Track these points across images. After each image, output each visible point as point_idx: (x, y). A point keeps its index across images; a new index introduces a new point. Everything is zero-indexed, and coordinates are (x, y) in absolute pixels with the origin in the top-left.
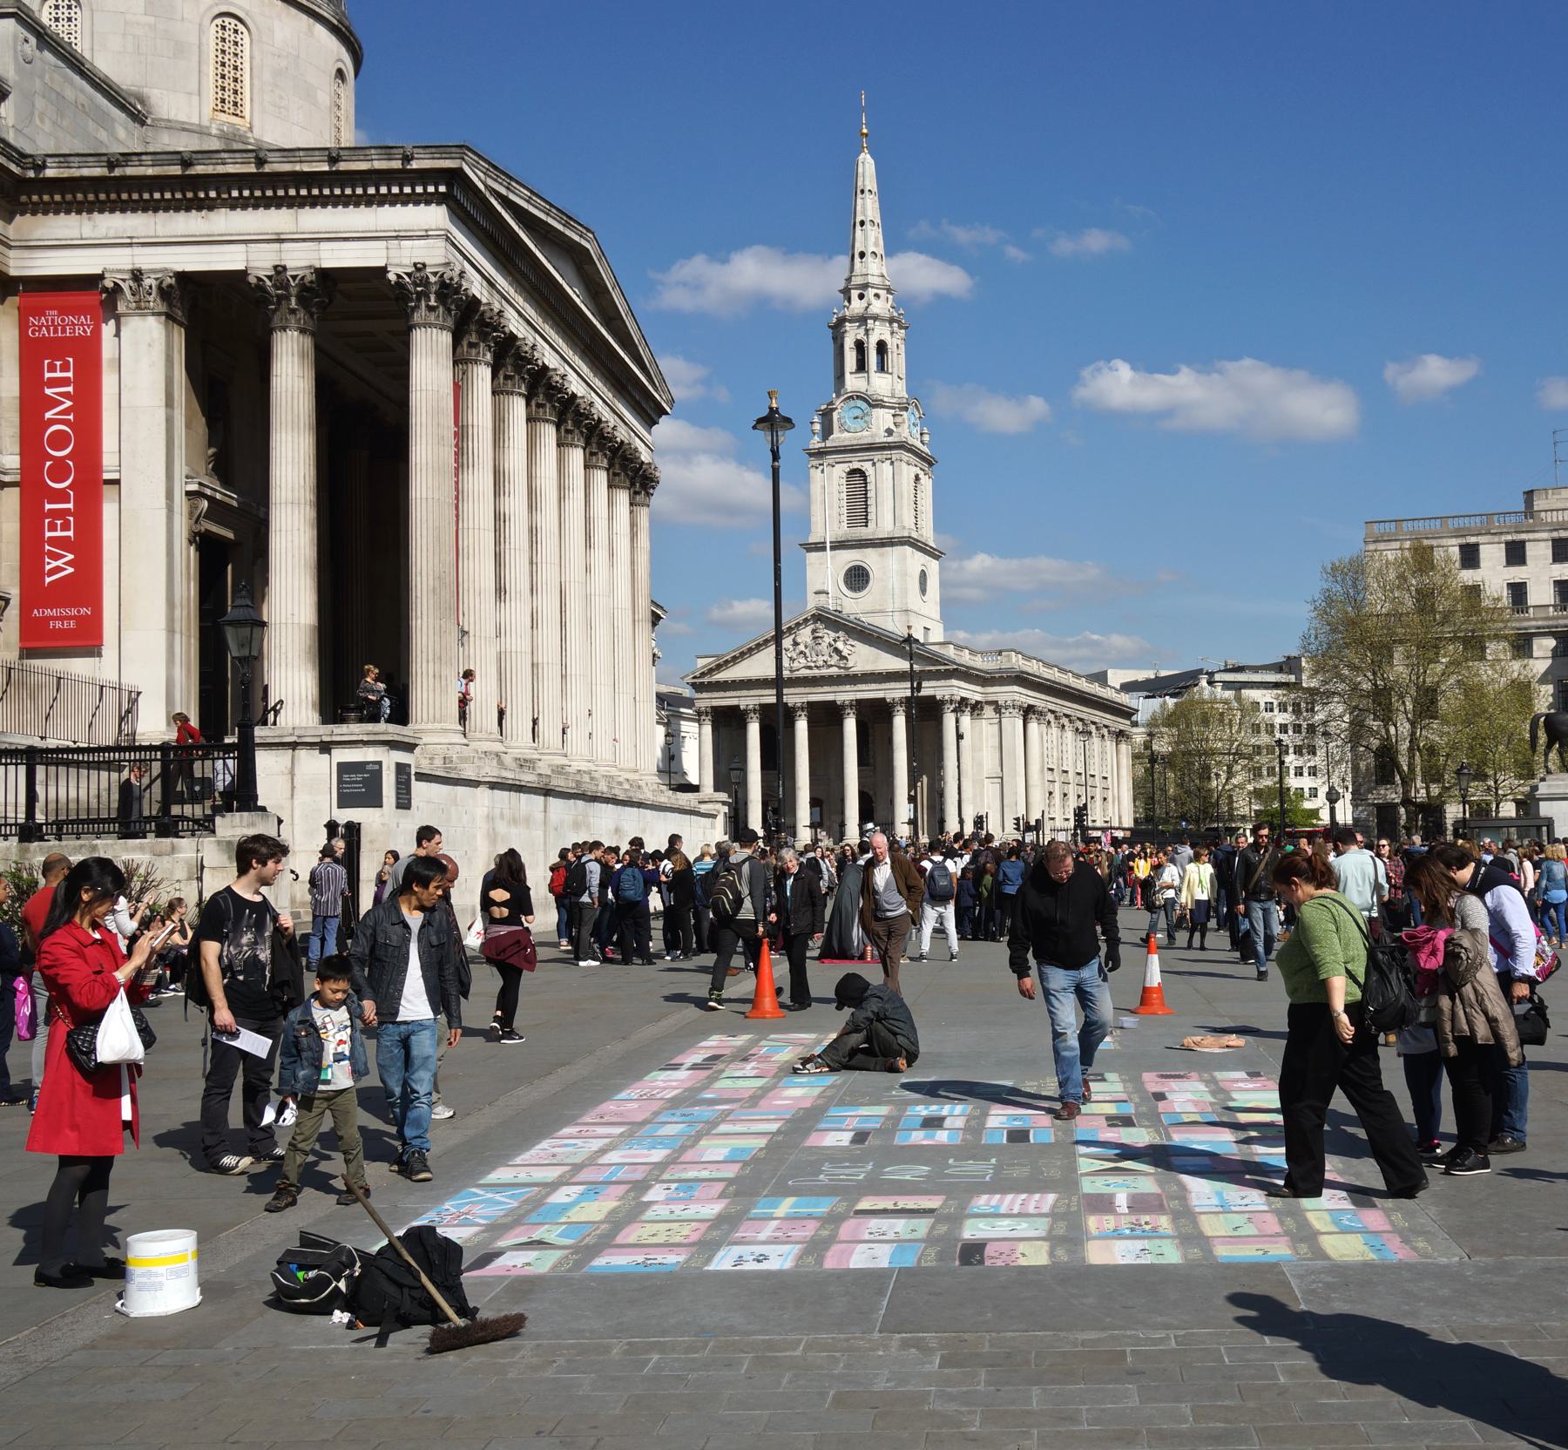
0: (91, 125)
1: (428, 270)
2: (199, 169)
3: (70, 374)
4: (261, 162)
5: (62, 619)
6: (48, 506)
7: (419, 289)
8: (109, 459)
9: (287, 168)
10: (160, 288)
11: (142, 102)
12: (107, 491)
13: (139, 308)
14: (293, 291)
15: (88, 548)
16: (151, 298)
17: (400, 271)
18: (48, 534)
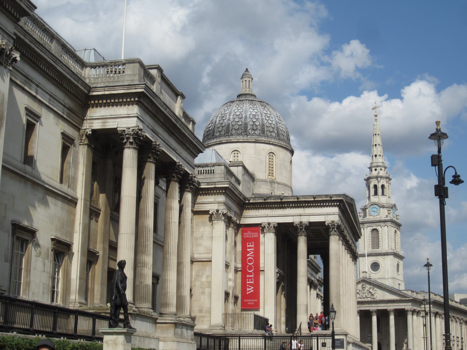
0: (249, 184)
1: (335, 222)
2: (284, 200)
3: (253, 246)
4: (298, 199)
5: (250, 302)
6: (248, 276)
8: (261, 265)
10: (274, 227)
13: (269, 231)
14: (304, 227)
16: (272, 229)
17: (328, 222)
18: (248, 282)
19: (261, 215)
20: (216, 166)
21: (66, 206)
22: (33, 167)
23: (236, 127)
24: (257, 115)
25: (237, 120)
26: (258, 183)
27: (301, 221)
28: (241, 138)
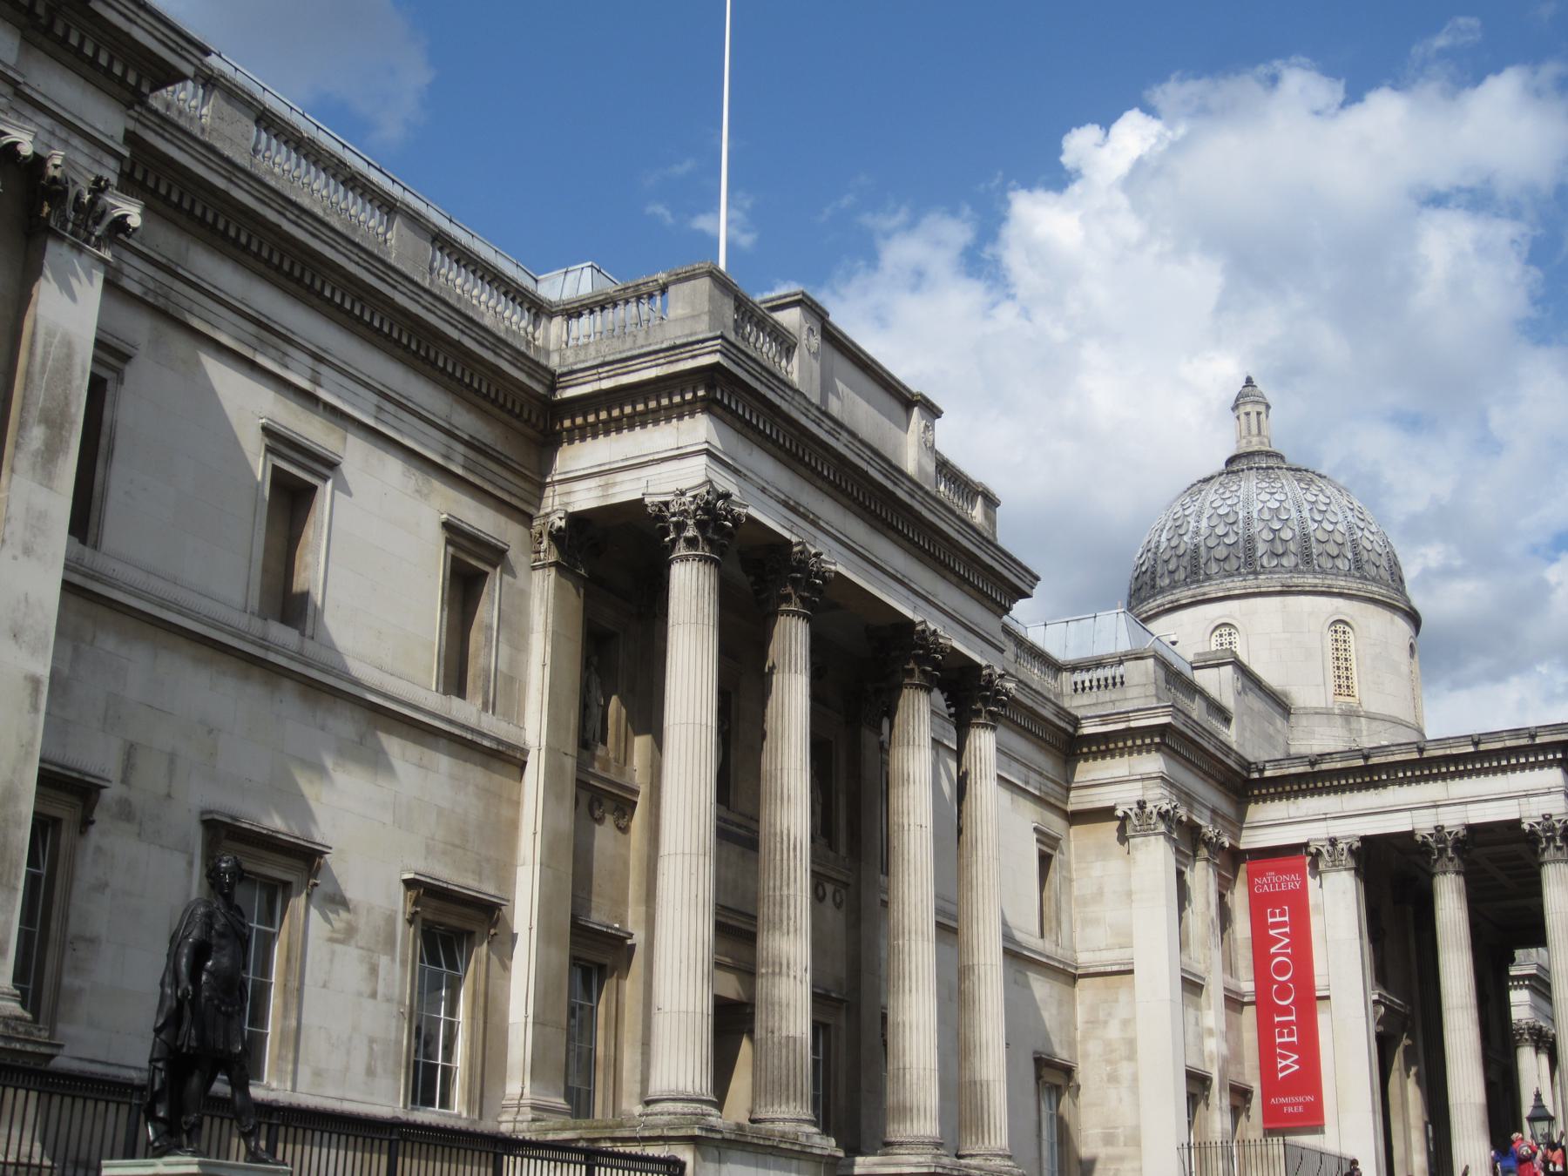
0: (1267, 724)
1: (1554, 818)
2: (1374, 761)
3: (1286, 919)
4: (1421, 750)
5: (1292, 1105)
6: (1277, 1019)
7: (1549, 834)
8: (1320, 981)
9: (1440, 752)
10: (1350, 850)
11: (1286, 697)
12: (1319, 1004)
13: (1335, 866)
14: (1450, 844)
15: (1308, 1049)
16: (1343, 858)
17: (1531, 821)
18: (1278, 1040)
19: (1306, 816)
20: (1128, 660)
21: (476, 774)
22: (309, 632)
23: (1221, 552)
24: (1285, 508)
25: (1220, 531)
26: (1304, 721)
27: (1440, 823)
28: (1236, 585)
